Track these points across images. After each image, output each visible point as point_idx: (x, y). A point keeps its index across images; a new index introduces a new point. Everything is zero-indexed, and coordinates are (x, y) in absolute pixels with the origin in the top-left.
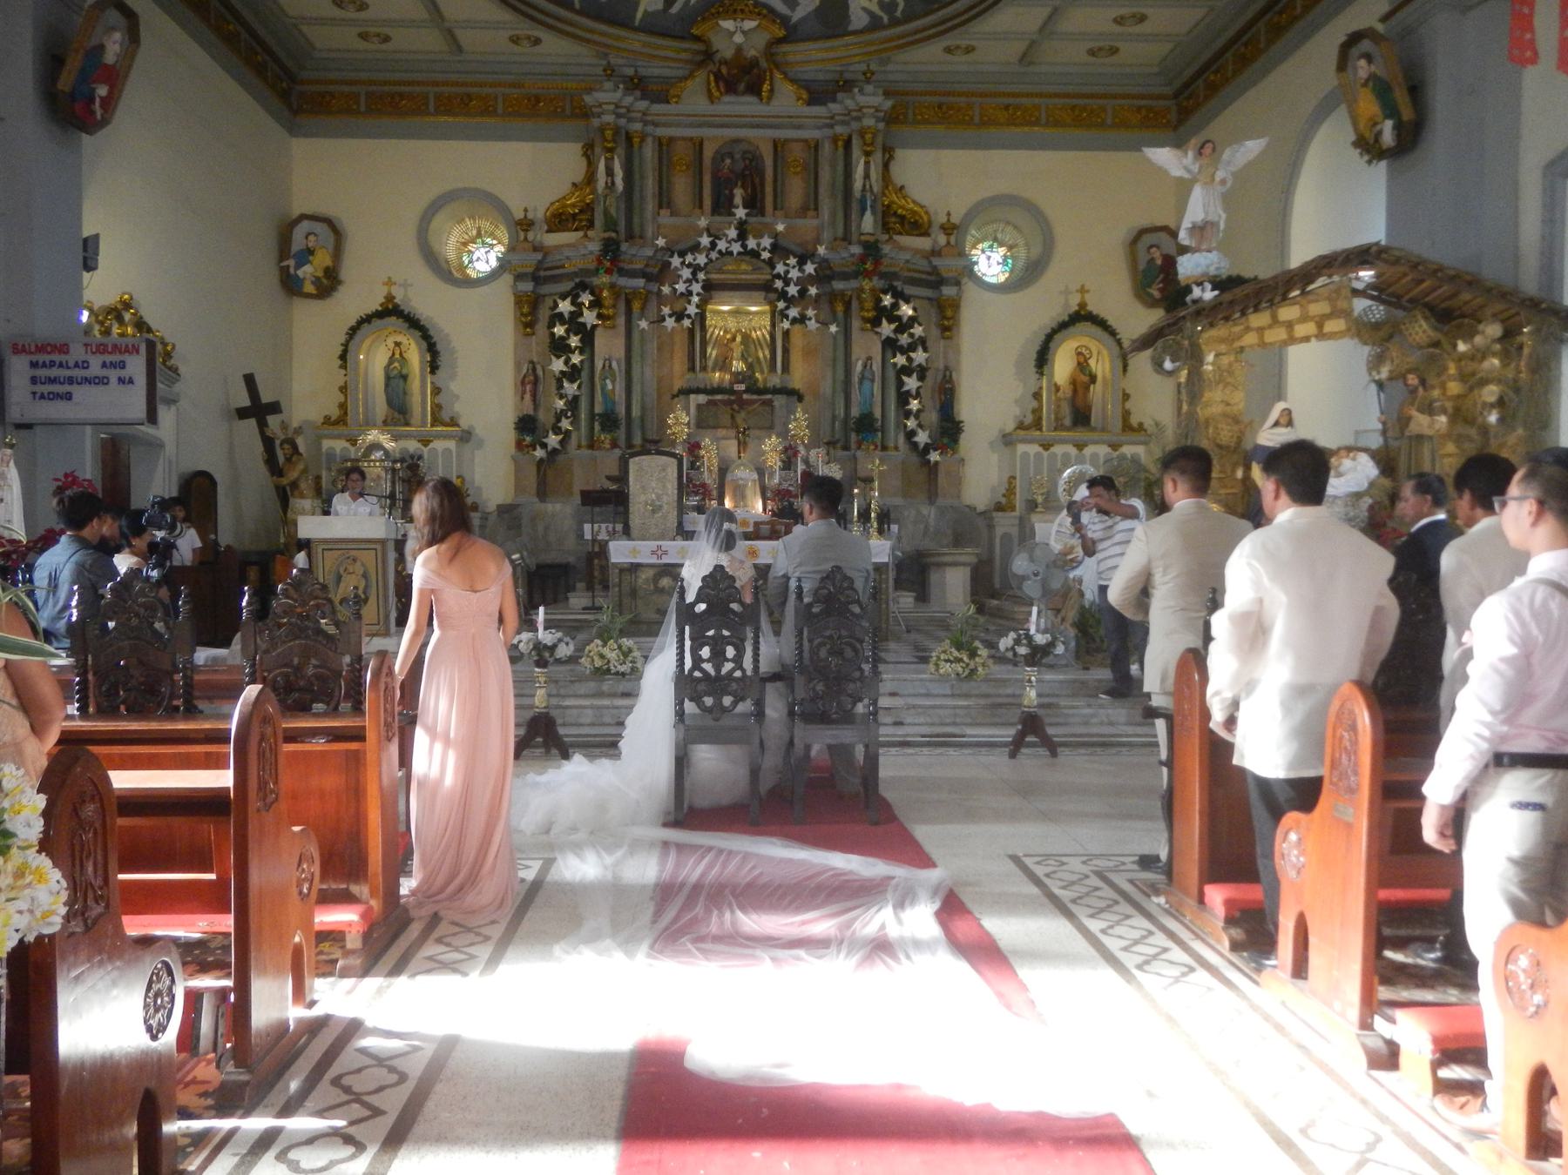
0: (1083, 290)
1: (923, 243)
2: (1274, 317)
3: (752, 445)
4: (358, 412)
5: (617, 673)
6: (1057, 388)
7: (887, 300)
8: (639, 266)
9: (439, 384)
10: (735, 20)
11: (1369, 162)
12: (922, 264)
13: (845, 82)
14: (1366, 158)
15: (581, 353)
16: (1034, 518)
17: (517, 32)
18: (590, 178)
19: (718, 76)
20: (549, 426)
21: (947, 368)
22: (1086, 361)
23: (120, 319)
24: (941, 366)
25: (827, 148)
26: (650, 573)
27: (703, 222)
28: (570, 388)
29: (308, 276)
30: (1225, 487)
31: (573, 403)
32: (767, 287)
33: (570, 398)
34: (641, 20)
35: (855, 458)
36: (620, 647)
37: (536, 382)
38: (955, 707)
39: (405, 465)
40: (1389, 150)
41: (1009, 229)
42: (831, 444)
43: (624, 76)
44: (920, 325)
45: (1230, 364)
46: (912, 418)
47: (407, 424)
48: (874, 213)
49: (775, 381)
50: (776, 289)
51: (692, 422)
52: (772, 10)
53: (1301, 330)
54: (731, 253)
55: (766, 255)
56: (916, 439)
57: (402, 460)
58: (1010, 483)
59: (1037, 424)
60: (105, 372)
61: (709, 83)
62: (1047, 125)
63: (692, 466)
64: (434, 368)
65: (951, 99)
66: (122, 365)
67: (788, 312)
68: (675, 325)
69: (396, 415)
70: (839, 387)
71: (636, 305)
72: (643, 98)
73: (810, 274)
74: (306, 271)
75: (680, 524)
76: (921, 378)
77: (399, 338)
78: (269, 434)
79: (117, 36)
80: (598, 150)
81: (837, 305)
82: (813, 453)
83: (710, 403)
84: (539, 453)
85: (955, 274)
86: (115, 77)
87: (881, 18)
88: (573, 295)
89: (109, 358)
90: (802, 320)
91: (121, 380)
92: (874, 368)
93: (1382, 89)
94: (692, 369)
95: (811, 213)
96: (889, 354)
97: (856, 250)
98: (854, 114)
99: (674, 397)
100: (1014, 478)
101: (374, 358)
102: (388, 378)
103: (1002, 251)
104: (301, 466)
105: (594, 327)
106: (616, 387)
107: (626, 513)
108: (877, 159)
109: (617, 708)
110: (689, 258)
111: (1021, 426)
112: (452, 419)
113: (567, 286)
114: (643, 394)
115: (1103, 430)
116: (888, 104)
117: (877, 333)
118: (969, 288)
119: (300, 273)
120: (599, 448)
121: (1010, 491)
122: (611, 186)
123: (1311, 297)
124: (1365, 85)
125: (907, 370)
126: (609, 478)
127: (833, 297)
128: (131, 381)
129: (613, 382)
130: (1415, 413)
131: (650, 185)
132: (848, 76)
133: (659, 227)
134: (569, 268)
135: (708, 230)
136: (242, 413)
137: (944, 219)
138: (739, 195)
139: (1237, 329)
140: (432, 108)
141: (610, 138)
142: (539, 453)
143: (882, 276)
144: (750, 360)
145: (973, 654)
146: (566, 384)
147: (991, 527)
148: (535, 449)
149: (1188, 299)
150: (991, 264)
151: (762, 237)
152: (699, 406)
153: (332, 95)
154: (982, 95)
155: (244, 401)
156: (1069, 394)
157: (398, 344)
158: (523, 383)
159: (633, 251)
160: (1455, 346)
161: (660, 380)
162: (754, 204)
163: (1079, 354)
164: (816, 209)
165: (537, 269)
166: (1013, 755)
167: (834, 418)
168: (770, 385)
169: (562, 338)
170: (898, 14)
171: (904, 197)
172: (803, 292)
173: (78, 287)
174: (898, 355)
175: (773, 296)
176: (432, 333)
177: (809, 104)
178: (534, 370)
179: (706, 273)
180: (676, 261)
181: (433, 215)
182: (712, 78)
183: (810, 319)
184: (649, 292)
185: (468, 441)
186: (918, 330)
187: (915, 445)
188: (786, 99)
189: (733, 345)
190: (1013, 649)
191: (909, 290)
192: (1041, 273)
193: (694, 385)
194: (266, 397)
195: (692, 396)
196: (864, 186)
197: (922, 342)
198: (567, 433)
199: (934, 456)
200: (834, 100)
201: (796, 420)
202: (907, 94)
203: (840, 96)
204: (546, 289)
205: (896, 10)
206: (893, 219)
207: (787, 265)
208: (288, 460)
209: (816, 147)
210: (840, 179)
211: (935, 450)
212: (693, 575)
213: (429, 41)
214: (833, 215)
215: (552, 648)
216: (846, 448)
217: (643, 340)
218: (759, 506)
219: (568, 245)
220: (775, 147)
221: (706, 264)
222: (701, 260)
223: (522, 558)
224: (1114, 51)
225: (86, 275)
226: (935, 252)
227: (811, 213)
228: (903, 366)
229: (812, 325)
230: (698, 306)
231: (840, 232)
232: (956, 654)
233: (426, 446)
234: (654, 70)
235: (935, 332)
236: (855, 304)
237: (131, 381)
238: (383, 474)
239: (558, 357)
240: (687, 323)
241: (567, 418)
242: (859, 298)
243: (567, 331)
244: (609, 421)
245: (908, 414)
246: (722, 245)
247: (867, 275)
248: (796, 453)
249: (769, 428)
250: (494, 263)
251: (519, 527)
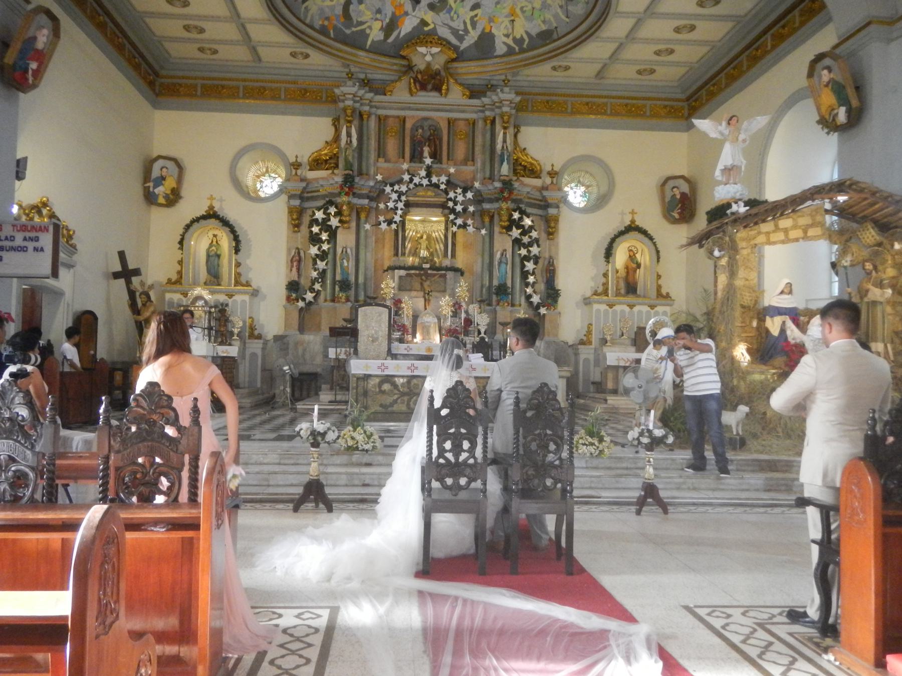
0: (633, 213)
2: (776, 226)
3: (433, 301)
4: (189, 276)
5: (363, 450)
6: (617, 272)
7: (516, 216)
8: (364, 192)
9: (239, 261)
10: (427, 47)
11: (828, 133)
12: (537, 195)
13: (492, 86)
14: (826, 130)
15: (328, 243)
16: (605, 349)
17: (294, 50)
18: (337, 138)
19: (416, 80)
20: (307, 288)
21: (551, 257)
22: (634, 255)
23: (39, 213)
24: (547, 256)
25: (480, 124)
26: (377, 380)
27: (405, 166)
28: (321, 265)
29: (161, 193)
30: (746, 332)
31: (323, 274)
32: (443, 206)
33: (321, 270)
34: (370, 46)
35: (495, 312)
36: (365, 432)
37: (299, 261)
38: (591, 477)
39: (217, 309)
40: (842, 125)
41: (587, 176)
42: (481, 302)
43: (359, 79)
44: (536, 231)
45: (748, 255)
46: (530, 287)
47: (219, 285)
48: (508, 163)
49: (447, 262)
50: (449, 208)
51: (396, 287)
52: (449, 43)
53: (774, 237)
54: (422, 185)
55: (443, 187)
56: (532, 300)
57: (216, 307)
58: (589, 328)
59: (605, 292)
60: (26, 244)
61: (410, 84)
62: (611, 114)
63: (396, 314)
64: (237, 250)
65: (554, 98)
66: (37, 239)
67: (455, 221)
68: (387, 227)
69: (212, 279)
70: (486, 266)
71: (363, 216)
72: (370, 91)
73: (469, 199)
74: (160, 190)
75: (389, 350)
76: (536, 263)
77: (216, 232)
78: (132, 288)
79: (45, 32)
80: (342, 121)
81: (486, 218)
82: (471, 307)
83: (408, 275)
84: (301, 304)
85: (556, 201)
86: (43, 57)
87: (514, 48)
88: (325, 208)
89: (28, 234)
90: (464, 226)
91: (36, 249)
92: (508, 256)
93: (838, 89)
94: (396, 254)
95: (470, 163)
96: (517, 248)
97: (498, 185)
98: (497, 104)
99: (385, 271)
100: (591, 324)
102: (208, 256)
103: (583, 189)
104: (152, 309)
105: (337, 227)
106: (350, 265)
107: (357, 341)
108: (511, 131)
109: (364, 474)
110: (396, 187)
111: (596, 293)
112: (247, 282)
113: (320, 203)
114: (366, 269)
115: (644, 297)
116: (518, 99)
117: (509, 235)
118: (564, 209)
119: (156, 191)
120: (339, 302)
121: (589, 332)
122: (349, 143)
123: (799, 214)
124: (827, 86)
125: (527, 258)
126: (345, 320)
127: (482, 213)
128: (42, 250)
129: (348, 261)
130: (870, 286)
131: (373, 144)
132: (495, 83)
133: (377, 169)
134: (322, 192)
135: (408, 171)
136: (116, 275)
137: (549, 168)
138: (426, 150)
139: (753, 233)
140: (241, 94)
141: (349, 115)
142: (301, 304)
143: (514, 201)
144: (431, 250)
145: (601, 440)
146: (319, 262)
147: (576, 354)
148: (298, 302)
149: (728, 212)
150: (576, 196)
151: (441, 176)
152: (400, 277)
153: (180, 85)
154: (573, 96)
155: (118, 268)
156: (624, 274)
157: (215, 236)
158: (292, 261)
159: (362, 182)
160: (893, 246)
161: (376, 261)
162: (434, 155)
163: (631, 250)
164: (473, 160)
165: (303, 192)
166: (638, 513)
167: (482, 286)
168: (444, 265)
169: (316, 234)
170: (525, 46)
171: (527, 155)
172: (465, 210)
173: (12, 191)
174: (522, 249)
175: (447, 211)
176: (236, 229)
177: (471, 97)
178: (299, 253)
179: (407, 196)
180: (388, 189)
181: (239, 159)
182: (412, 81)
183: (469, 226)
184: (371, 208)
185: (256, 296)
186: (534, 234)
187: (531, 303)
188: (456, 95)
189: (421, 241)
190: (638, 439)
191: (529, 210)
192: (607, 203)
193: (398, 264)
194: (131, 266)
195: (396, 271)
196: (503, 147)
197: (537, 241)
198: (318, 293)
199: (543, 311)
200: (485, 96)
201: (460, 286)
202: (530, 94)
203: (488, 93)
204: (307, 205)
205: (524, 44)
206: (520, 167)
207: (456, 193)
208: (144, 305)
209: (474, 123)
210: (488, 143)
211: (544, 306)
213: (240, 54)
214: (484, 164)
215: (323, 435)
216: (490, 304)
217: (366, 237)
218: (437, 338)
219: (322, 178)
220: (449, 123)
221: (406, 191)
222: (404, 188)
223: (290, 369)
224: (652, 71)
225: (17, 183)
227: (470, 163)
228: (525, 255)
229: (471, 229)
230: (401, 217)
231: (488, 175)
232: (590, 440)
233: (230, 298)
235: (544, 236)
236: (496, 217)
237: (42, 250)
238: (203, 315)
239: (314, 245)
240: (394, 226)
241: (319, 283)
242: (499, 214)
243: (320, 230)
244: (345, 285)
245: (527, 285)
246: (416, 180)
247: (505, 200)
248: (460, 307)
250: (276, 188)
251: (287, 348)
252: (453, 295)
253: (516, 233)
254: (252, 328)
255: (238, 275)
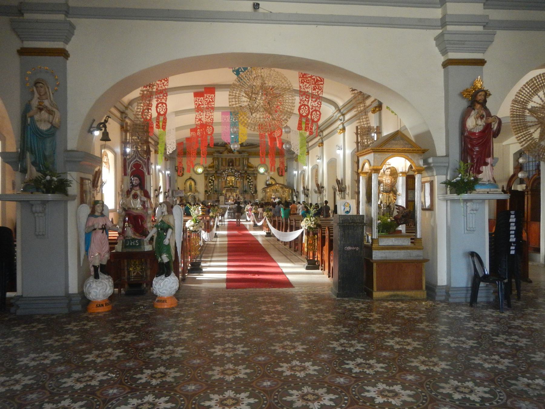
1: (253, 169)
18: (213, 162)
31: (212, 189)
32: (234, 176)
42: (241, 194)
49: (235, 186)
88: (212, 176)
101: (188, 184)
106: (217, 187)
118: (259, 175)
125: (250, 185)
127: (242, 176)
131: (220, 163)
150: (262, 170)
162: (232, 165)
197: (252, 182)
212: (228, 207)
219: (211, 171)
226: (254, 171)
234: (221, 150)
244: (216, 191)
249: (235, 191)
252: (236, 192)
253: (248, 180)
254: (199, 199)
255: (196, 190)
